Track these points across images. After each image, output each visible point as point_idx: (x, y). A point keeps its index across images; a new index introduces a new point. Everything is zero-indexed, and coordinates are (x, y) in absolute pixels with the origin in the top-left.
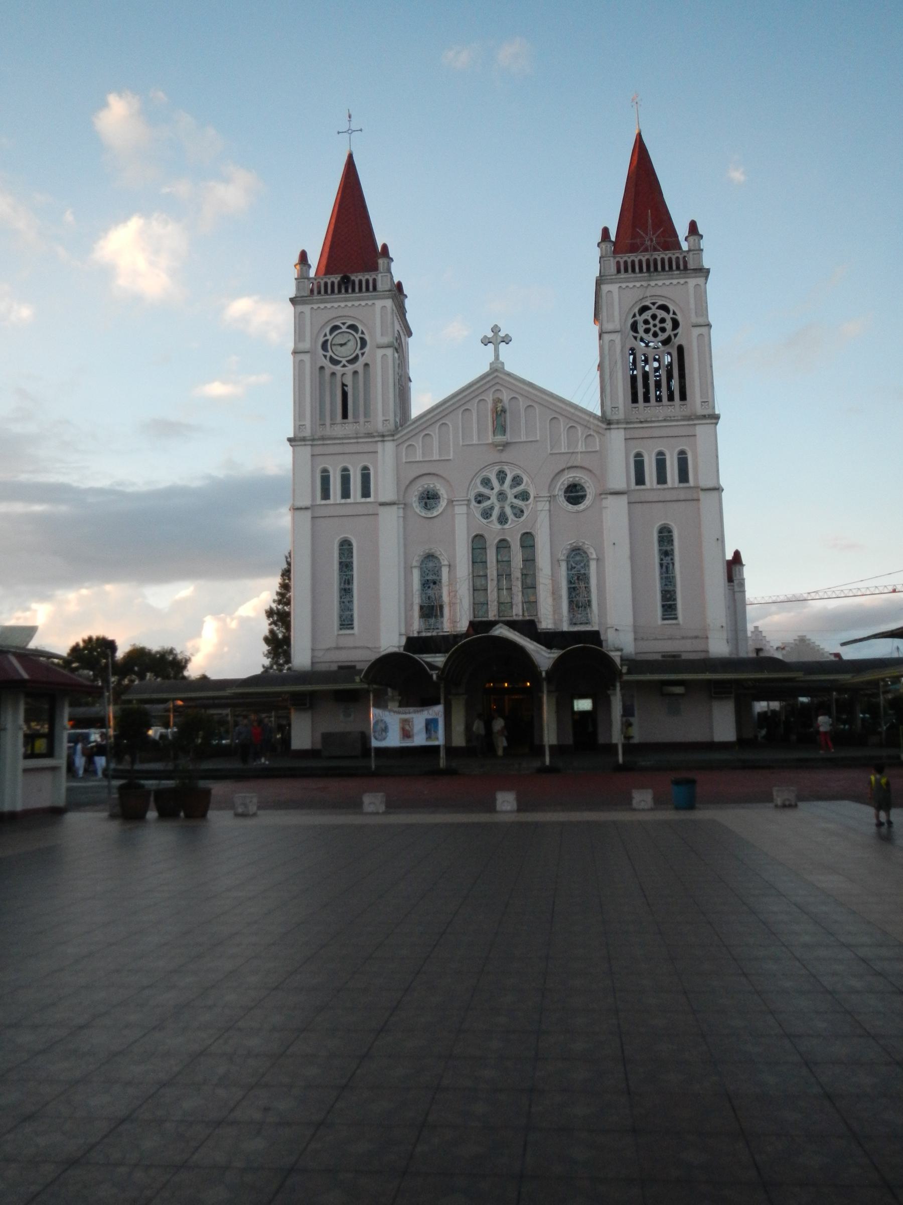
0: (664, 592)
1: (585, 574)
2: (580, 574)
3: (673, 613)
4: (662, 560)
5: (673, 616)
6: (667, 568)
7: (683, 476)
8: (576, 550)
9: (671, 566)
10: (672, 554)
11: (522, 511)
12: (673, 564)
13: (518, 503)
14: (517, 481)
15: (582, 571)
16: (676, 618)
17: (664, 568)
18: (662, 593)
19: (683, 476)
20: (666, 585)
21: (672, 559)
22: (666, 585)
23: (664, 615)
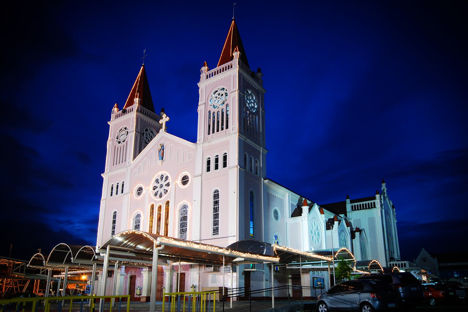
0: (214, 221)
1: (186, 216)
2: (185, 216)
3: (217, 231)
4: (214, 206)
5: (217, 233)
6: (216, 209)
7: (225, 165)
8: (184, 205)
9: (218, 208)
10: (218, 203)
11: (167, 191)
12: (218, 207)
13: (166, 188)
14: (167, 178)
15: (185, 215)
16: (218, 234)
17: (215, 209)
18: (213, 222)
19: (225, 165)
20: (215, 218)
21: (218, 205)
22: (215, 218)
23: (213, 233)
